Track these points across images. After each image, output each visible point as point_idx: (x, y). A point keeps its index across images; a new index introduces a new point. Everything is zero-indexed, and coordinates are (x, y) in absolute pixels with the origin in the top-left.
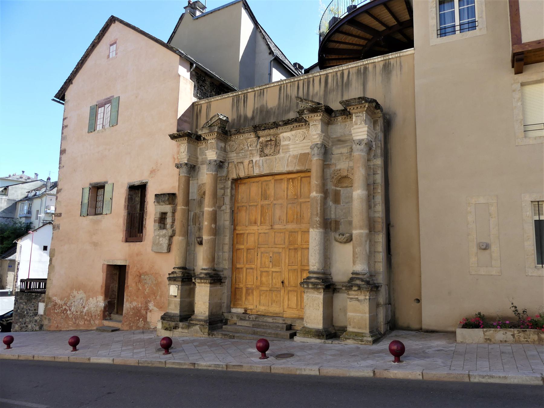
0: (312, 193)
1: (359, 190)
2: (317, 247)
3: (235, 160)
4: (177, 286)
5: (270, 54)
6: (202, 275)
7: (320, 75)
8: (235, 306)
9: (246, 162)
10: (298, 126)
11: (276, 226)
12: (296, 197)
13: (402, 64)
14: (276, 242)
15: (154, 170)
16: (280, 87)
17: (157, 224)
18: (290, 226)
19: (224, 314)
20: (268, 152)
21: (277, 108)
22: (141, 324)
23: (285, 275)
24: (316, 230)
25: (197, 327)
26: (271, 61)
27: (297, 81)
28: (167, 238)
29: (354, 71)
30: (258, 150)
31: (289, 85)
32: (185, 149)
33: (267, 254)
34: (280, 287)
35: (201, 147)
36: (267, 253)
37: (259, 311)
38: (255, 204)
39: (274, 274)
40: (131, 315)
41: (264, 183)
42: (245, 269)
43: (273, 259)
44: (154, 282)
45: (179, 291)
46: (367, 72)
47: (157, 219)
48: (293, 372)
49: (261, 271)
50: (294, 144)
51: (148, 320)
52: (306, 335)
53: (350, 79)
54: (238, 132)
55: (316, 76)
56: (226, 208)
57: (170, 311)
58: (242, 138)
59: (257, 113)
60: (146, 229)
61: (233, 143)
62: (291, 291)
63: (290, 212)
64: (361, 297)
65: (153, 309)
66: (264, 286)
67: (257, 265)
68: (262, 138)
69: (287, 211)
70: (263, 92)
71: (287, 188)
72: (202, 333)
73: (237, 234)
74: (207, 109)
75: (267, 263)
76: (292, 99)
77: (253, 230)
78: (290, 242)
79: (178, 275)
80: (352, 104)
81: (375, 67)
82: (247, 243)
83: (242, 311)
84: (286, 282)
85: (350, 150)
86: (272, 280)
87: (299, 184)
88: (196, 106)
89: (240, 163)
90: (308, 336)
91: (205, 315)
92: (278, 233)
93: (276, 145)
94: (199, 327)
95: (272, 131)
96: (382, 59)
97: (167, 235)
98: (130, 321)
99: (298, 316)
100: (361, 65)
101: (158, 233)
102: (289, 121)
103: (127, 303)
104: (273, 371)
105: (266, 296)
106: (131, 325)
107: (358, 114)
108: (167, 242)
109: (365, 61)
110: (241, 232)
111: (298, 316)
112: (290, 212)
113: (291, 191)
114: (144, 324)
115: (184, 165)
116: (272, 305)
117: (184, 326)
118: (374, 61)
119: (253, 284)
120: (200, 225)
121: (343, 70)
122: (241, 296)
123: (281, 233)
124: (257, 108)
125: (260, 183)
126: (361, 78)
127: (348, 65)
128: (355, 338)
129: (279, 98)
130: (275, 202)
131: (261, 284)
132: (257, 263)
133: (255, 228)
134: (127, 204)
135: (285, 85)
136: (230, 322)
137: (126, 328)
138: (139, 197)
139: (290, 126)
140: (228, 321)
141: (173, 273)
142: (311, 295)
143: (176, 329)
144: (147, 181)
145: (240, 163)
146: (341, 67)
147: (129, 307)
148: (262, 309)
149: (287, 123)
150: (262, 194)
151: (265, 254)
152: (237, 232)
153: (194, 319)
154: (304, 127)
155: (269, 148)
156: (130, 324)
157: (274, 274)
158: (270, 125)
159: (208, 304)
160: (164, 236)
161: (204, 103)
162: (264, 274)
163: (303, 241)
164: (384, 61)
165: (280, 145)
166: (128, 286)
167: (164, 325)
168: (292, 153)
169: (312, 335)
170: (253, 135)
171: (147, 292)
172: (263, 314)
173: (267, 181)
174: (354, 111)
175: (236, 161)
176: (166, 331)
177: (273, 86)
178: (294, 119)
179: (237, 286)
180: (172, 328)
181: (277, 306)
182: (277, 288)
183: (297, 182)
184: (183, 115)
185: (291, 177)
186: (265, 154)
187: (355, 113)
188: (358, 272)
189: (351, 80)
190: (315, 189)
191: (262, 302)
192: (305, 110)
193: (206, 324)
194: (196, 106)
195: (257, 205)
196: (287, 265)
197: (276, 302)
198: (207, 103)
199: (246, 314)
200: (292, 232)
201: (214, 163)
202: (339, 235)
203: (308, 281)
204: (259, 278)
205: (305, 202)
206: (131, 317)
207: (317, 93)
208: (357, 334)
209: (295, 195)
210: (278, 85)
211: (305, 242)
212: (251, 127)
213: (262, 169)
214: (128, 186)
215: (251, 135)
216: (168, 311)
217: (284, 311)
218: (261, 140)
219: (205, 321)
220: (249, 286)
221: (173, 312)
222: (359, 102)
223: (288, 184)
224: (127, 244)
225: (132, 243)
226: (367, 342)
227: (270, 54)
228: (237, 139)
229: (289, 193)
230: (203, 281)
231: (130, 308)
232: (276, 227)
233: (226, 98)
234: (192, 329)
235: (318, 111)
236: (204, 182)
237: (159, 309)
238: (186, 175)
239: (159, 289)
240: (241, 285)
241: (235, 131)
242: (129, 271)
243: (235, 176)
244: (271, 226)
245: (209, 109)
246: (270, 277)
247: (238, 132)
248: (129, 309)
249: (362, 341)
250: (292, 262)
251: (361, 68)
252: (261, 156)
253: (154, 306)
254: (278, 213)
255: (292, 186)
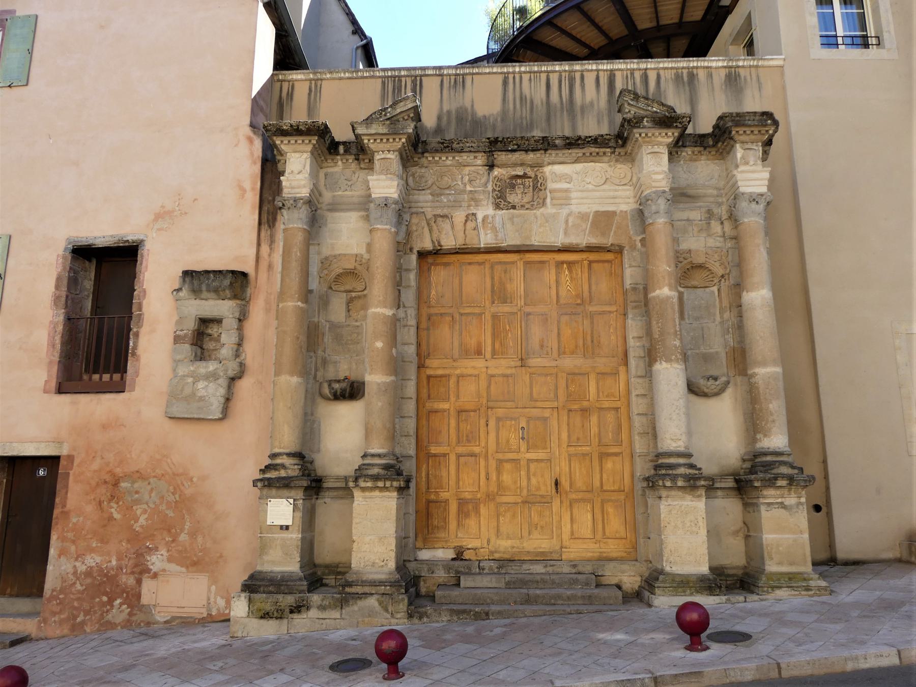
0: (660, 288)
1: (763, 288)
2: (681, 401)
3: (429, 209)
4: (291, 501)
5: (354, 33)
6: (375, 471)
7: (598, 71)
8: (428, 543)
9: (459, 216)
10: (594, 154)
11: (534, 360)
12: (579, 301)
13: (762, 80)
14: (535, 395)
15: (170, 213)
16: (505, 77)
17: (187, 347)
18: (568, 363)
19: (408, 565)
20: (516, 200)
21: (499, 119)
22: (119, 612)
23: (562, 468)
24: (676, 365)
25: (372, 602)
26: (357, 48)
27: (545, 72)
28: (223, 382)
29: (670, 76)
30: (489, 194)
31: (526, 77)
32: (305, 166)
33: (513, 422)
34: (549, 493)
35: (330, 170)
36: (512, 419)
37: (496, 552)
38: (477, 311)
39: (533, 466)
40: (79, 592)
41: (498, 268)
42: (453, 458)
43: (528, 433)
44: (171, 498)
45: (299, 514)
46: (696, 82)
47: (186, 335)
48: (838, 669)
49: (497, 460)
50: (582, 191)
51: (145, 600)
52: (680, 590)
53: (662, 89)
54: (447, 147)
55: (588, 71)
56: (406, 314)
57: (267, 568)
58: (449, 162)
59: (449, 122)
60: (138, 360)
61: (423, 170)
62: (577, 501)
63: (567, 332)
64: (791, 501)
65: (164, 570)
66: (506, 493)
67: (486, 447)
68: (500, 170)
69: (558, 329)
70: (463, 82)
71: (557, 282)
72: (389, 616)
73: (429, 377)
74: (309, 94)
75: (513, 441)
76: (535, 106)
77: (473, 367)
78: (569, 395)
79: (289, 472)
80: (746, 122)
81: (710, 76)
82: (458, 397)
83: (451, 554)
84: (565, 483)
85: (707, 215)
86: (529, 479)
87: (587, 275)
88: (278, 84)
89: (442, 216)
90: (684, 592)
91: (386, 570)
92: (539, 375)
93: (535, 188)
94: (378, 600)
95: (531, 157)
96: (725, 64)
97: (222, 374)
98: (75, 608)
99: (598, 554)
100: (683, 68)
101: (192, 368)
102: (578, 140)
103: (63, 559)
104: (785, 674)
105: (514, 516)
106: (79, 620)
107: (749, 146)
108: (222, 391)
109: (693, 61)
110: (440, 372)
111: (596, 555)
112: (567, 332)
113: (568, 287)
114: (130, 614)
115: (304, 203)
116: (529, 534)
117: (326, 603)
118: (709, 65)
119: (477, 489)
120: (325, 352)
121: (646, 69)
122: (445, 520)
123: (547, 375)
124: (449, 112)
125: (487, 266)
126: (685, 91)
127: (660, 62)
128: (791, 585)
129: (504, 99)
130: (528, 309)
131: (499, 489)
132: (487, 443)
133: (480, 363)
134: (64, 294)
135: (517, 76)
136: (425, 583)
137: (54, 630)
138: (91, 280)
139: (576, 152)
140: (419, 582)
141: (268, 468)
142: (677, 503)
143: (299, 612)
144: (141, 237)
145: (442, 216)
146: (645, 62)
147: (71, 570)
148: (505, 545)
149: (573, 143)
150: (493, 291)
151: (508, 422)
152: (430, 372)
153: (358, 581)
154: (606, 159)
155: (519, 191)
156: (75, 617)
157: (533, 466)
158: (532, 142)
159: (393, 542)
160: (212, 377)
161: (302, 80)
162: (508, 466)
163: (601, 394)
164: (727, 69)
165: (545, 189)
166: (66, 514)
167: (258, 605)
168: (575, 208)
169: (693, 590)
170: (481, 159)
171: (142, 526)
172: (507, 556)
173: (505, 263)
174: (743, 138)
175: (430, 213)
176: (263, 621)
177: (489, 73)
178: (590, 137)
179: (433, 497)
180: (288, 610)
181: (546, 537)
182: (542, 496)
183: (580, 270)
184: (259, 93)
185: (566, 260)
186: (510, 203)
187: (743, 142)
188: (778, 450)
189: (665, 91)
190: (667, 282)
191: (503, 529)
192: (645, 119)
193: (398, 590)
194: (279, 83)
195: (480, 314)
196: (565, 446)
197: (542, 527)
198: (311, 80)
199: (462, 560)
200: (574, 374)
201: (394, 206)
202: (708, 379)
203: (671, 472)
204: (494, 476)
205: (603, 313)
206: (78, 599)
207: (592, 103)
208: (791, 576)
209: (577, 296)
210: (501, 73)
211: (607, 396)
212: (484, 140)
213: (500, 235)
214: (70, 246)
215: (475, 157)
216: (259, 568)
217: (562, 548)
218: (496, 173)
219: (393, 584)
220: (467, 496)
221: (277, 569)
222: (760, 120)
223: (558, 274)
224: (66, 398)
225: (82, 395)
226: (819, 590)
227: (354, 33)
228: (437, 162)
229: (563, 293)
230: (380, 484)
231: (75, 573)
232: (534, 362)
233: (366, 77)
234: (356, 608)
235: (675, 125)
236: (338, 252)
237: (187, 568)
238: (305, 227)
239: (186, 516)
240: (444, 495)
241: (439, 143)
242: (71, 472)
243: (428, 245)
244: (522, 359)
245: (316, 94)
246: (523, 473)
247: (445, 147)
248: (71, 577)
249: (808, 589)
250: (578, 439)
251: (682, 73)
252: (497, 206)
253: (170, 560)
254: (536, 332)
255: (567, 278)
